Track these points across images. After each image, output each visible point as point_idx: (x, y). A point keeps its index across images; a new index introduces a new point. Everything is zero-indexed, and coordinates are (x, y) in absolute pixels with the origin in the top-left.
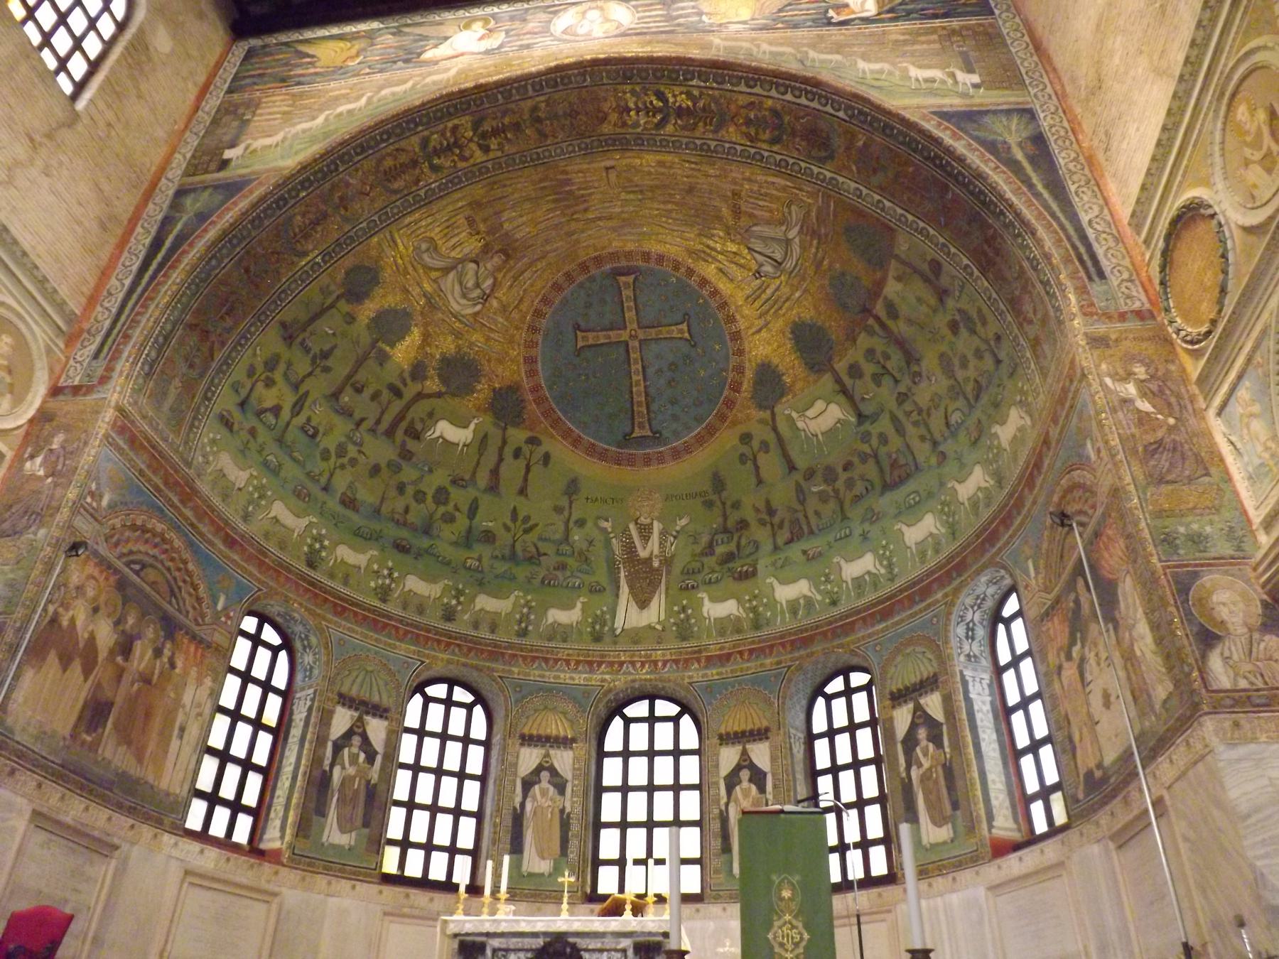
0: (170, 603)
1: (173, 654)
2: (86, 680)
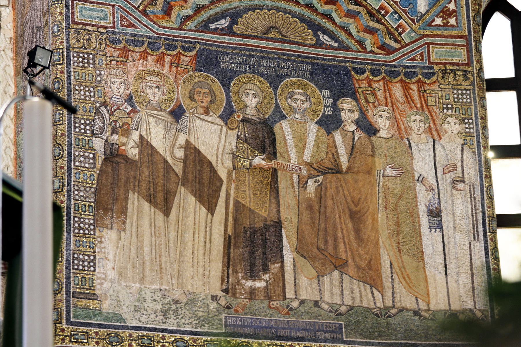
0: (320, 45)
1: (363, 113)
2: (211, 210)
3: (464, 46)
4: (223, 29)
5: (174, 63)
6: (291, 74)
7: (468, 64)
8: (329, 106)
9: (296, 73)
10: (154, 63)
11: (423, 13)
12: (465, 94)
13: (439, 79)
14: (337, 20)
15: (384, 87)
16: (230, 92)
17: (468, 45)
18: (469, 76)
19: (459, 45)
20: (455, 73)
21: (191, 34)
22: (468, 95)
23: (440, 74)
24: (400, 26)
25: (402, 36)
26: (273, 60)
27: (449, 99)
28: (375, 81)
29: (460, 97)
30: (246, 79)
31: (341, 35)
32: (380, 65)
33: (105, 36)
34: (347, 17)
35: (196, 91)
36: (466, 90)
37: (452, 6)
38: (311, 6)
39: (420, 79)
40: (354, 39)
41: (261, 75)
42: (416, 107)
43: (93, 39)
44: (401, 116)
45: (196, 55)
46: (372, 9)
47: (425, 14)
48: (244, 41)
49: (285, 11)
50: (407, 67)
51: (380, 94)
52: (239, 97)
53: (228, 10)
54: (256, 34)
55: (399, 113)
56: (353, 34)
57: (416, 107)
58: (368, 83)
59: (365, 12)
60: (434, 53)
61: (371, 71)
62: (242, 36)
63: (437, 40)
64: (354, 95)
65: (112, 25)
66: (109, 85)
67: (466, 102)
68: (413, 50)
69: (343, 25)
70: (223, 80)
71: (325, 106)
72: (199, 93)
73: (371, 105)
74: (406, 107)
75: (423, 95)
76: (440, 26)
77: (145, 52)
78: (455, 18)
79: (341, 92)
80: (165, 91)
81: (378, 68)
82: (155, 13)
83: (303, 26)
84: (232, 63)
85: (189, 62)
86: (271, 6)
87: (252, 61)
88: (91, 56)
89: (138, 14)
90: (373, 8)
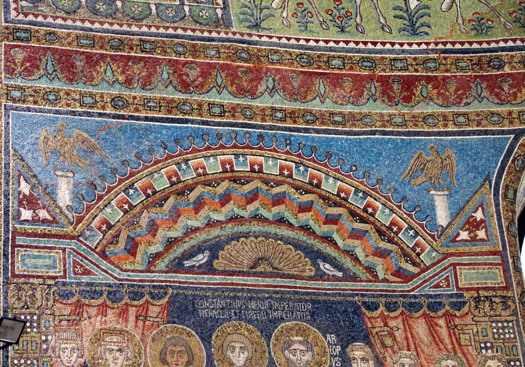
0: (321, 276)
3: (499, 264)
4: (200, 266)
5: (140, 316)
6: (287, 317)
7: (506, 288)
8: (336, 356)
9: (292, 315)
10: (115, 319)
11: (445, 226)
12: (506, 327)
13: (473, 310)
14: (340, 243)
15: (404, 325)
16: (211, 348)
17: (504, 263)
18: (510, 303)
19: (492, 264)
20: (491, 300)
21: (162, 276)
22: (511, 328)
23: (473, 303)
24: (417, 245)
25: (421, 257)
26: (263, 301)
27: (487, 335)
28: (391, 318)
29: (501, 331)
30: (231, 328)
31: (346, 262)
32: (396, 296)
33: (53, 290)
34: (352, 238)
35: (168, 350)
36: (508, 322)
37: (479, 215)
38: (307, 228)
39: (447, 311)
40: (362, 265)
41: (250, 322)
42: (446, 349)
43: (38, 295)
44: (428, 362)
45: (167, 302)
46: (381, 226)
47: (446, 228)
48: (227, 279)
49: (276, 237)
50: (430, 296)
51: (399, 335)
52: (222, 353)
53: (205, 242)
54: (242, 269)
55: (426, 359)
56: (360, 259)
57: (446, 349)
58: (383, 322)
59: (374, 230)
60: (463, 277)
61: (386, 306)
62: (224, 273)
63: (465, 259)
64: (366, 339)
65: (62, 274)
66: (57, 353)
67: (510, 338)
68: (436, 275)
69: (348, 249)
70: (202, 333)
71: (331, 356)
72: (173, 352)
73: (389, 349)
74: (433, 349)
75: (454, 332)
76: (466, 241)
77: (104, 305)
78: (484, 230)
79: (350, 335)
80: (129, 355)
81: (394, 300)
82: (116, 254)
83: (299, 254)
84: (213, 309)
85: (160, 312)
86: (259, 232)
87: (238, 304)
88: (35, 318)
89: (95, 257)
90: (382, 225)
